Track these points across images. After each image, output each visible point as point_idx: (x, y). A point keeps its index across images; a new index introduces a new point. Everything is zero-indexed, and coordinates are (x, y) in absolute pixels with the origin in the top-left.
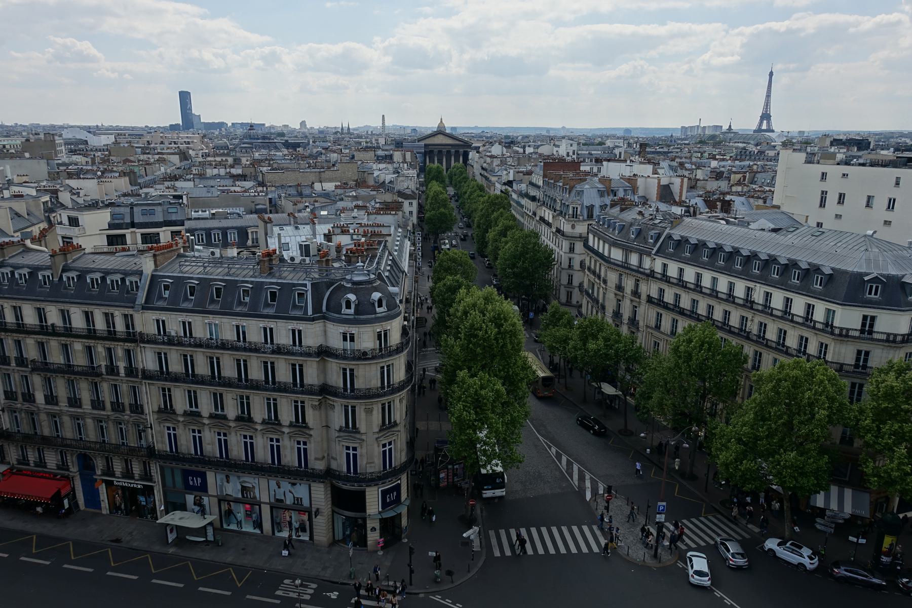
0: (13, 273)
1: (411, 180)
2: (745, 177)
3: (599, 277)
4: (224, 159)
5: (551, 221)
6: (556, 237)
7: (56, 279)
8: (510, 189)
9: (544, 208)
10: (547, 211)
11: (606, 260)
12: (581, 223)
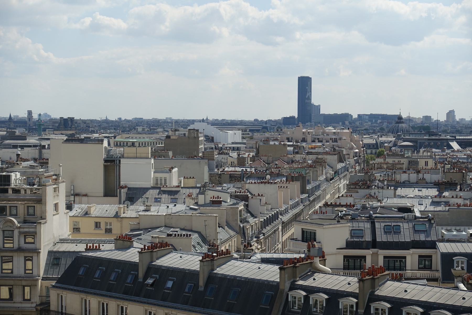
0: (307, 298)
4: (396, 160)
7: (361, 311)
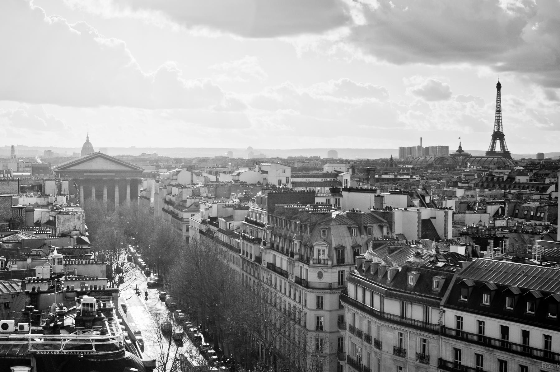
1: (79, 218)
2: (503, 209)
3: (368, 338)
5: (284, 268)
6: (295, 290)
8: (213, 228)
9: (273, 252)
10: (279, 256)
11: (381, 316)
12: (330, 270)
